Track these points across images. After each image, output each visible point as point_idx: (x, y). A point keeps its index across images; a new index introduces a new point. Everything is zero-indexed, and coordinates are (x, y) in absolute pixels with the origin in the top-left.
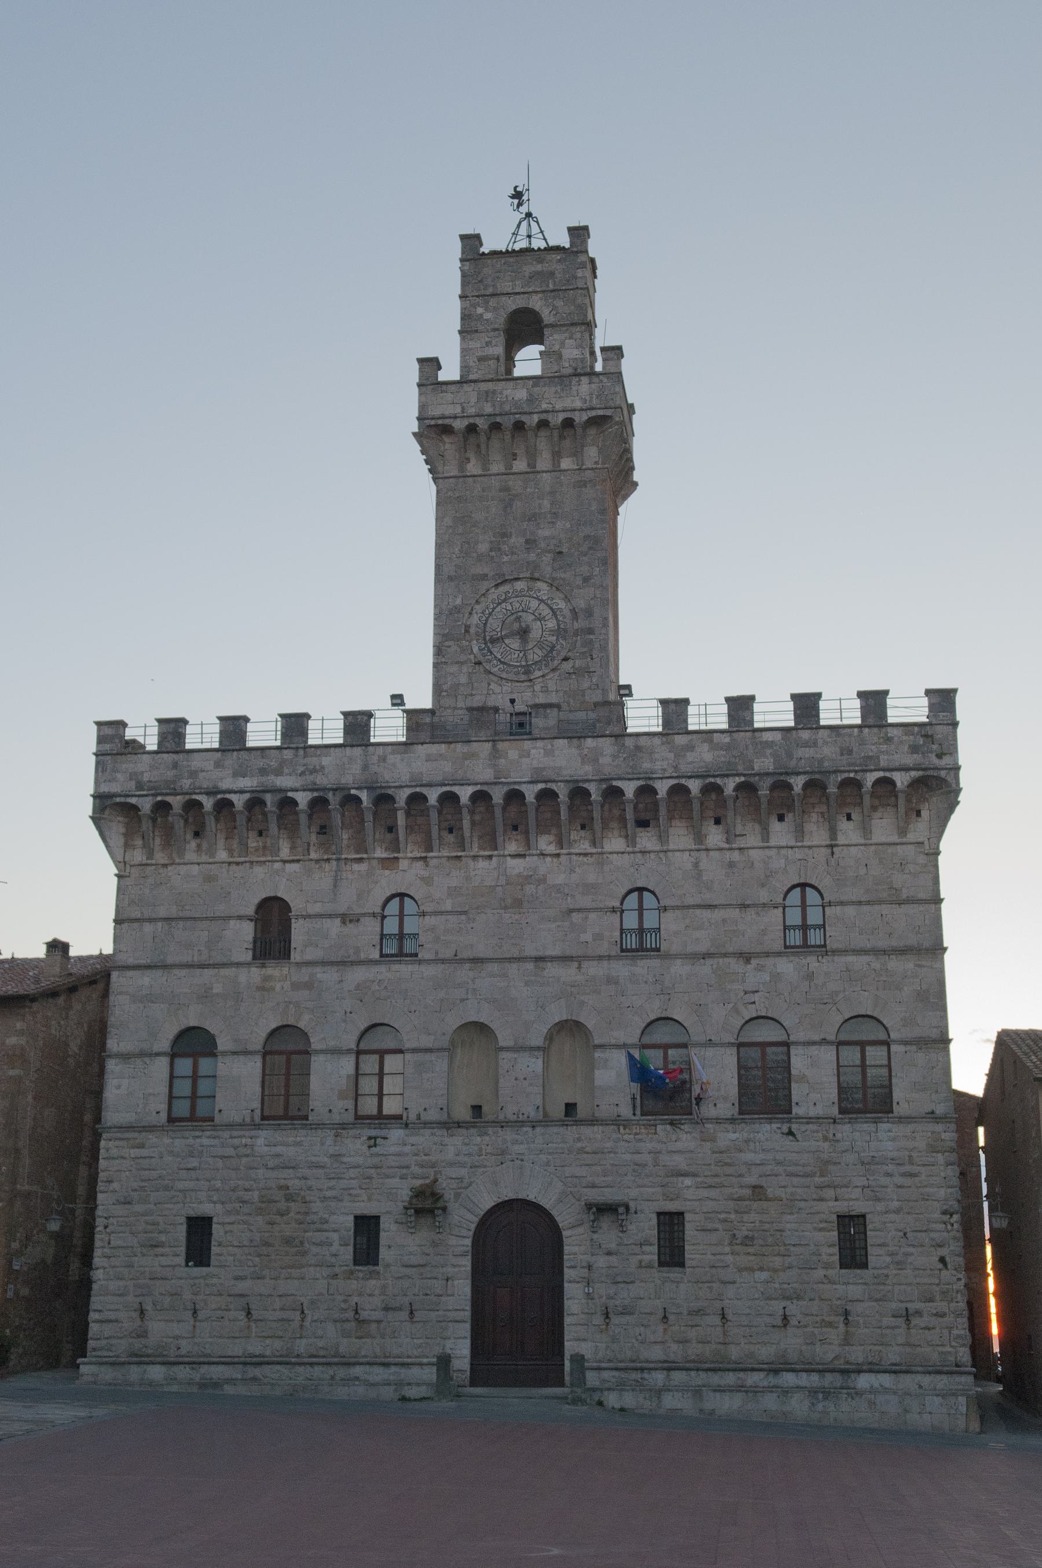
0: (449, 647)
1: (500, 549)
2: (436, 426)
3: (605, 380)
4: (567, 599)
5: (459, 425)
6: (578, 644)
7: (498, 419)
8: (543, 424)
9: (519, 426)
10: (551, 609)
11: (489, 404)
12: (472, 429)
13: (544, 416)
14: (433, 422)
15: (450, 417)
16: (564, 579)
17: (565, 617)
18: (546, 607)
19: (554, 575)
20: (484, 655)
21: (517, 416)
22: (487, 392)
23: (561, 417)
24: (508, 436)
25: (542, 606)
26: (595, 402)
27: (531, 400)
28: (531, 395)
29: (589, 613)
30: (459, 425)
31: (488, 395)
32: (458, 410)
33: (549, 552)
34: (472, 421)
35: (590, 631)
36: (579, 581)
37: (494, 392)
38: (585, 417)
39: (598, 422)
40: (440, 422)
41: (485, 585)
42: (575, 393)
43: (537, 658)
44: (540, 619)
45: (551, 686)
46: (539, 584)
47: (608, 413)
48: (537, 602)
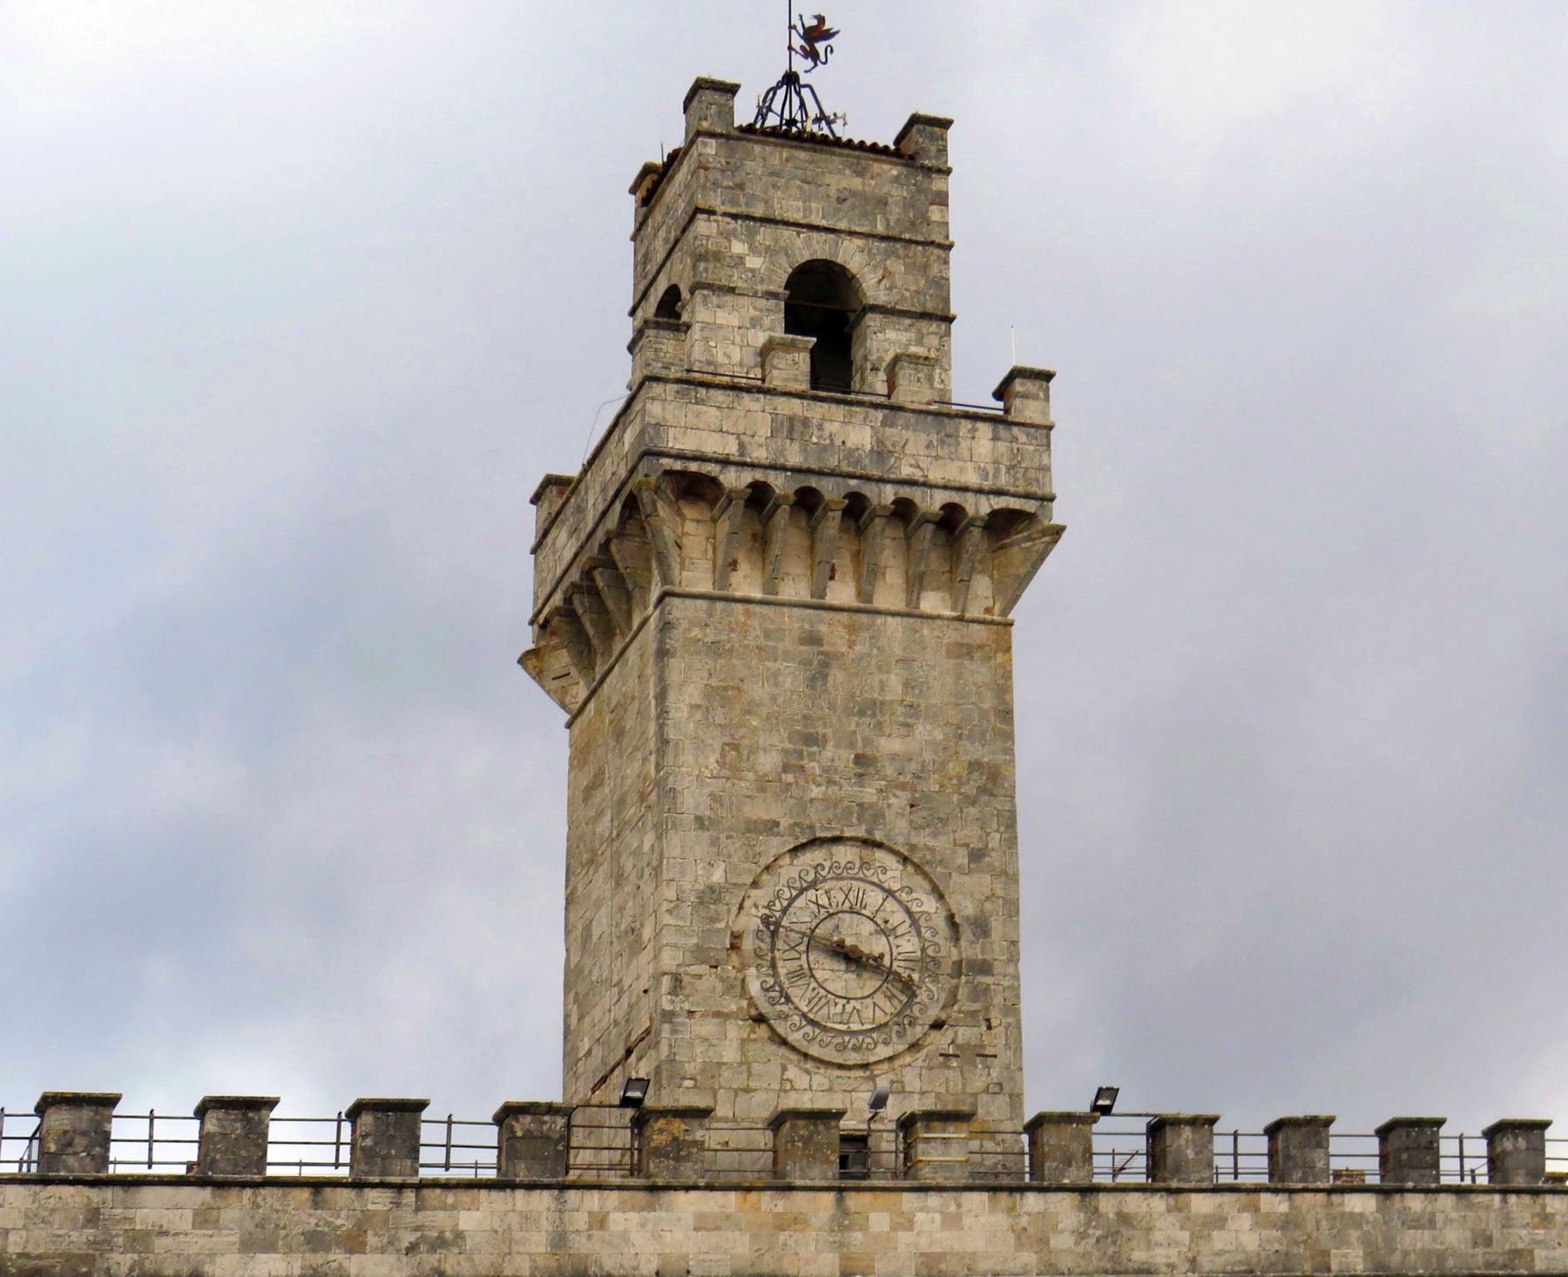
0: (700, 977)
1: (802, 768)
2: (683, 474)
3: (1023, 438)
4: (941, 897)
5: (734, 480)
6: (962, 993)
7: (813, 482)
8: (903, 511)
9: (856, 508)
10: (908, 911)
11: (796, 446)
12: (759, 496)
13: (906, 492)
14: (678, 465)
15: (717, 461)
16: (932, 850)
17: (935, 933)
18: (896, 907)
19: (914, 840)
20: (773, 1002)
21: (853, 482)
22: (791, 419)
23: (939, 499)
24: (832, 524)
25: (891, 905)
26: (1003, 481)
27: (881, 453)
28: (880, 442)
29: (981, 927)
30: (734, 480)
31: (792, 428)
32: (732, 449)
33: (903, 787)
34: (759, 475)
35: (985, 968)
36: (962, 858)
37: (806, 422)
38: (981, 507)
39: (1004, 524)
40: (693, 467)
41: (775, 845)
42: (966, 455)
43: (881, 1018)
44: (886, 931)
45: (912, 1080)
46: (880, 855)
47: (1030, 506)
48: (880, 895)
